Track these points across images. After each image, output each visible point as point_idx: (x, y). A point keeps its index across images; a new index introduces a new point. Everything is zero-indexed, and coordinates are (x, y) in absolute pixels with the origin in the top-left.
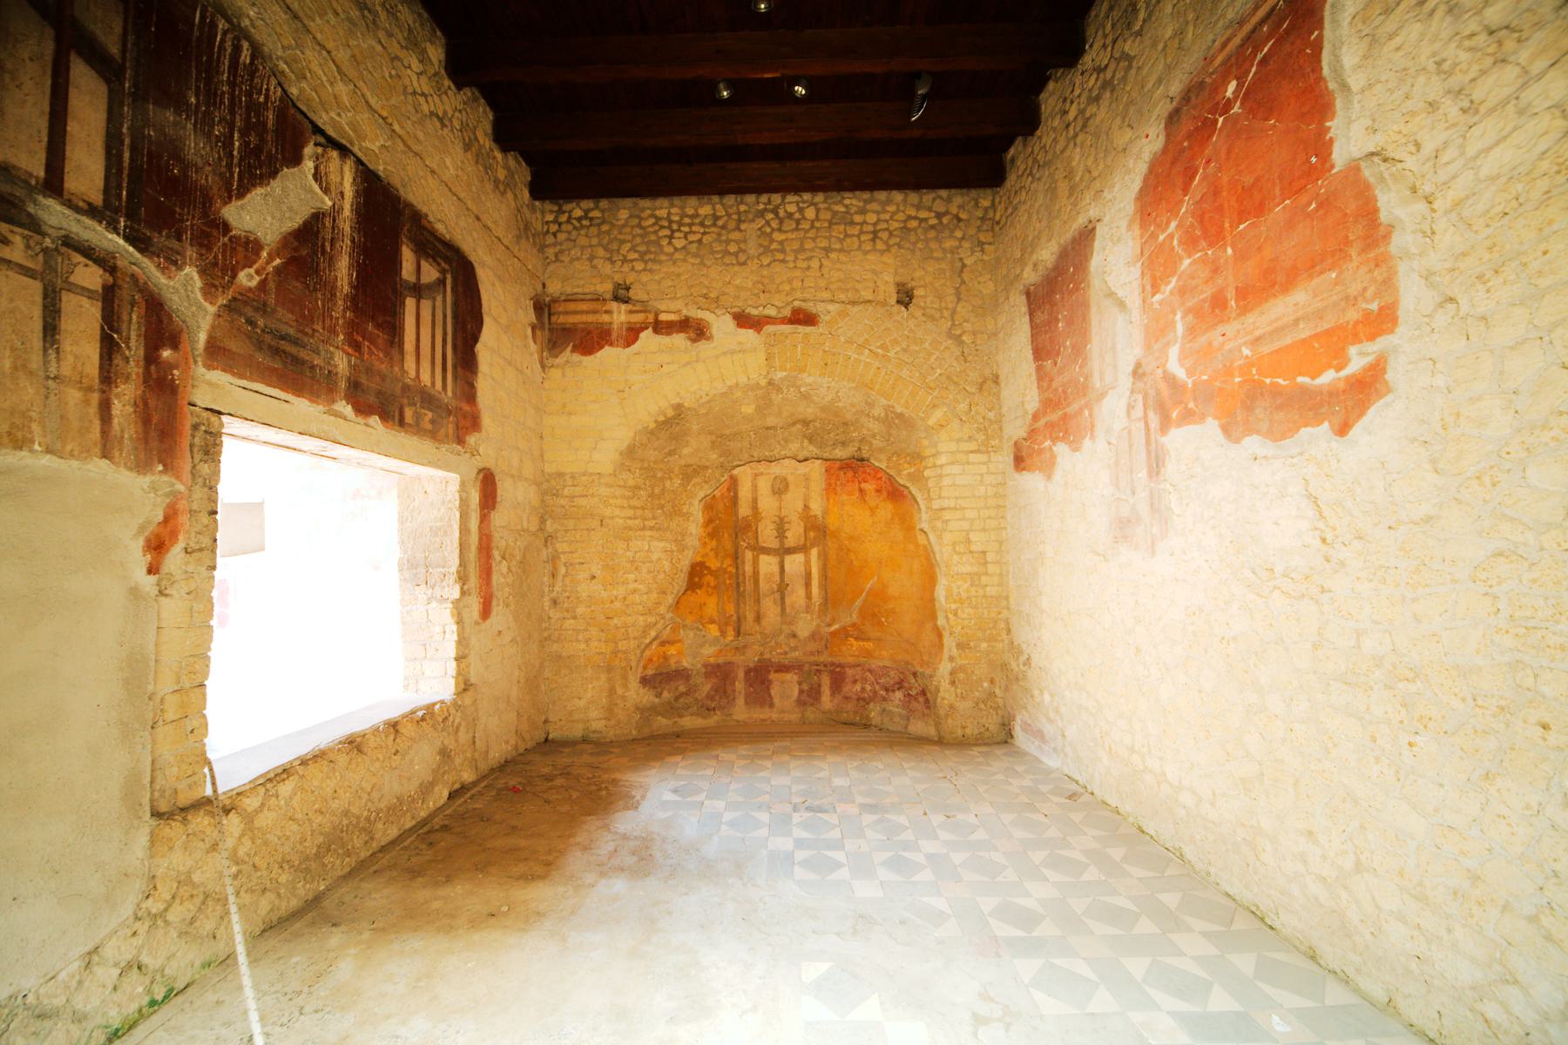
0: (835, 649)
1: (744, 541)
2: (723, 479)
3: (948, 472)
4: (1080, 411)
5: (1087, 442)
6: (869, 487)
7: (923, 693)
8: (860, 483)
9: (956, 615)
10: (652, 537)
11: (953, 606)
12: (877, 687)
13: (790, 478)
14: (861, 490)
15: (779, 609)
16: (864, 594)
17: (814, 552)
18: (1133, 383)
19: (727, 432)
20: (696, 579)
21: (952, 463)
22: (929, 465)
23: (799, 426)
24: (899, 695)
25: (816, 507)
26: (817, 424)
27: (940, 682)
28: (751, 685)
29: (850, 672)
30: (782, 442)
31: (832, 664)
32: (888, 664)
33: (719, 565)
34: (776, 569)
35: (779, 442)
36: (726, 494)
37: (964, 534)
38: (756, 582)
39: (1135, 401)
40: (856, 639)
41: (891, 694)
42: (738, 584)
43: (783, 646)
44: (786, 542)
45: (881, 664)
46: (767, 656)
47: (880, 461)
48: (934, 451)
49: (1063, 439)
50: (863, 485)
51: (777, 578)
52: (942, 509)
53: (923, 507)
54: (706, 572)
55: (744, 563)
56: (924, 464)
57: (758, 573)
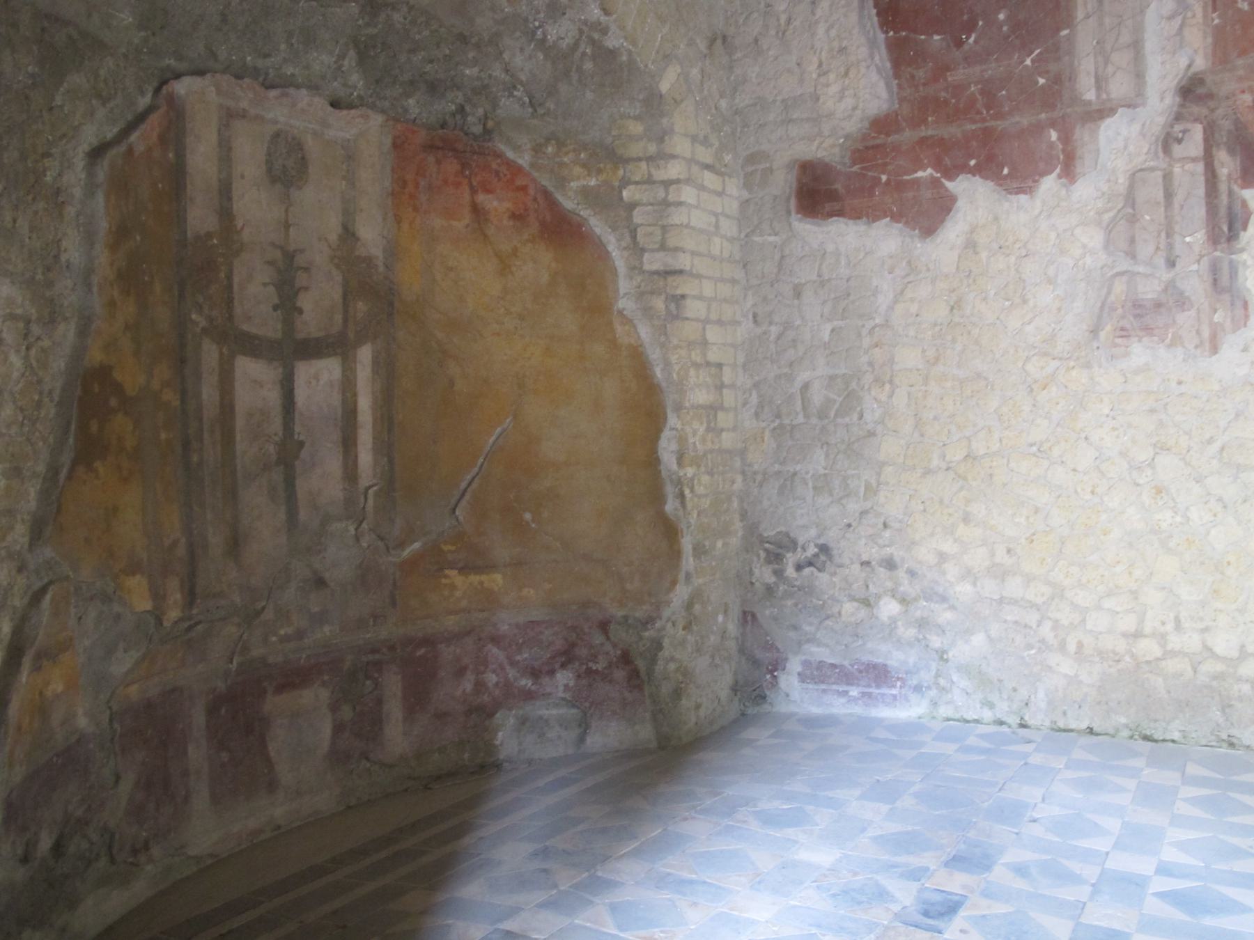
4: (1038, 129)
5: (1049, 184)
6: (496, 204)
7: (626, 658)
9: (692, 490)
12: (512, 673)
13: (311, 146)
14: (476, 209)
15: (282, 515)
17: (365, 354)
18: (1182, 106)
20: (94, 427)
24: (564, 678)
25: (371, 234)
27: (663, 628)
29: (447, 653)
34: (273, 396)
38: (228, 439)
39: (1184, 132)
41: (545, 680)
42: (186, 445)
45: (521, 619)
46: (256, 652)
47: (517, 148)
48: (652, 148)
49: (977, 171)
50: (481, 198)
51: (276, 426)
52: (668, 273)
56: (621, 172)
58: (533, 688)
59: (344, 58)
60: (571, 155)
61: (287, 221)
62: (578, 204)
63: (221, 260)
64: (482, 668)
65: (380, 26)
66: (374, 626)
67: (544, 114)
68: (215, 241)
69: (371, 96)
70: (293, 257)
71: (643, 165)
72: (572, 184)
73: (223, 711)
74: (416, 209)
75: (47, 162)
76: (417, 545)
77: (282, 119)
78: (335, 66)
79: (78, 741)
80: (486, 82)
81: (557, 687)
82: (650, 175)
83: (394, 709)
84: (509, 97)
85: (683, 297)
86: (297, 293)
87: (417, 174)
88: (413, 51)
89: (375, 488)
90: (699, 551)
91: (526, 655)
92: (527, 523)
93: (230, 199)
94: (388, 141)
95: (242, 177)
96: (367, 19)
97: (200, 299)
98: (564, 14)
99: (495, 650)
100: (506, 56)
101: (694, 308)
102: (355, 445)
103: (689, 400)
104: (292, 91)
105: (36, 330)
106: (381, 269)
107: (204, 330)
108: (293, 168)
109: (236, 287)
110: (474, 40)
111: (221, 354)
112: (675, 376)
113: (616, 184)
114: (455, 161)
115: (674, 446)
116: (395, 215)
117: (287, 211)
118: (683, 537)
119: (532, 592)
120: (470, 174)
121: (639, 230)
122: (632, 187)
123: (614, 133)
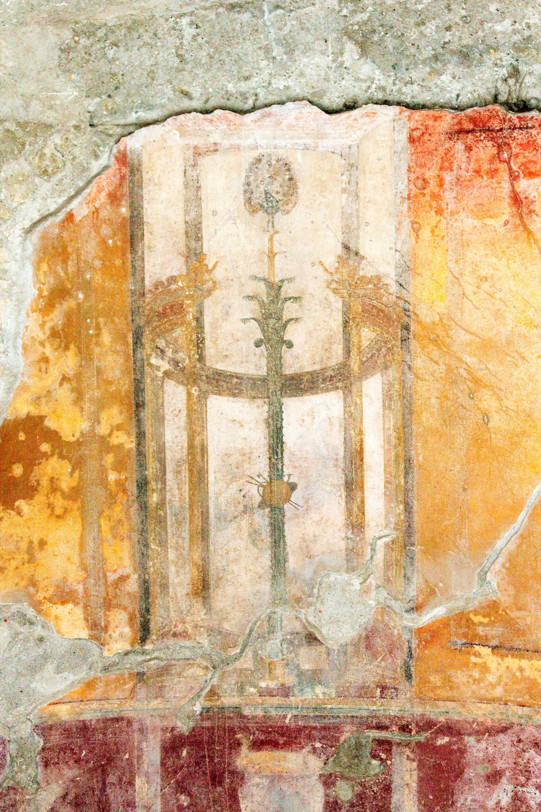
0: (435, 679)
2: (95, 166)
8: (514, 177)
15: (266, 559)
16: (523, 516)
28: (181, 788)
30: (277, 51)
33: (85, 426)
35: (267, 50)
36: (104, 214)
40: (494, 648)
43: (279, 671)
44: (288, 355)
54: (45, 447)
55: (160, 419)
57: (204, 450)
59: (342, 54)
61: (271, 251)
64: (522, 779)
65: (370, 9)
66: (382, 697)
68: (180, 284)
69: (394, 84)
73: (184, 753)
74: (439, 212)
77: (262, 142)
78: (334, 65)
80: (527, 33)
86: (285, 326)
87: (441, 169)
93: (199, 239)
94: (404, 137)
95: (214, 213)
96: (351, 6)
97: (162, 343)
102: (362, 488)
104: (275, 108)
106: (394, 288)
107: (167, 374)
108: (277, 193)
109: (207, 328)
111: (189, 394)
114: (490, 144)
116: (413, 223)
117: (271, 240)
120: (510, 158)
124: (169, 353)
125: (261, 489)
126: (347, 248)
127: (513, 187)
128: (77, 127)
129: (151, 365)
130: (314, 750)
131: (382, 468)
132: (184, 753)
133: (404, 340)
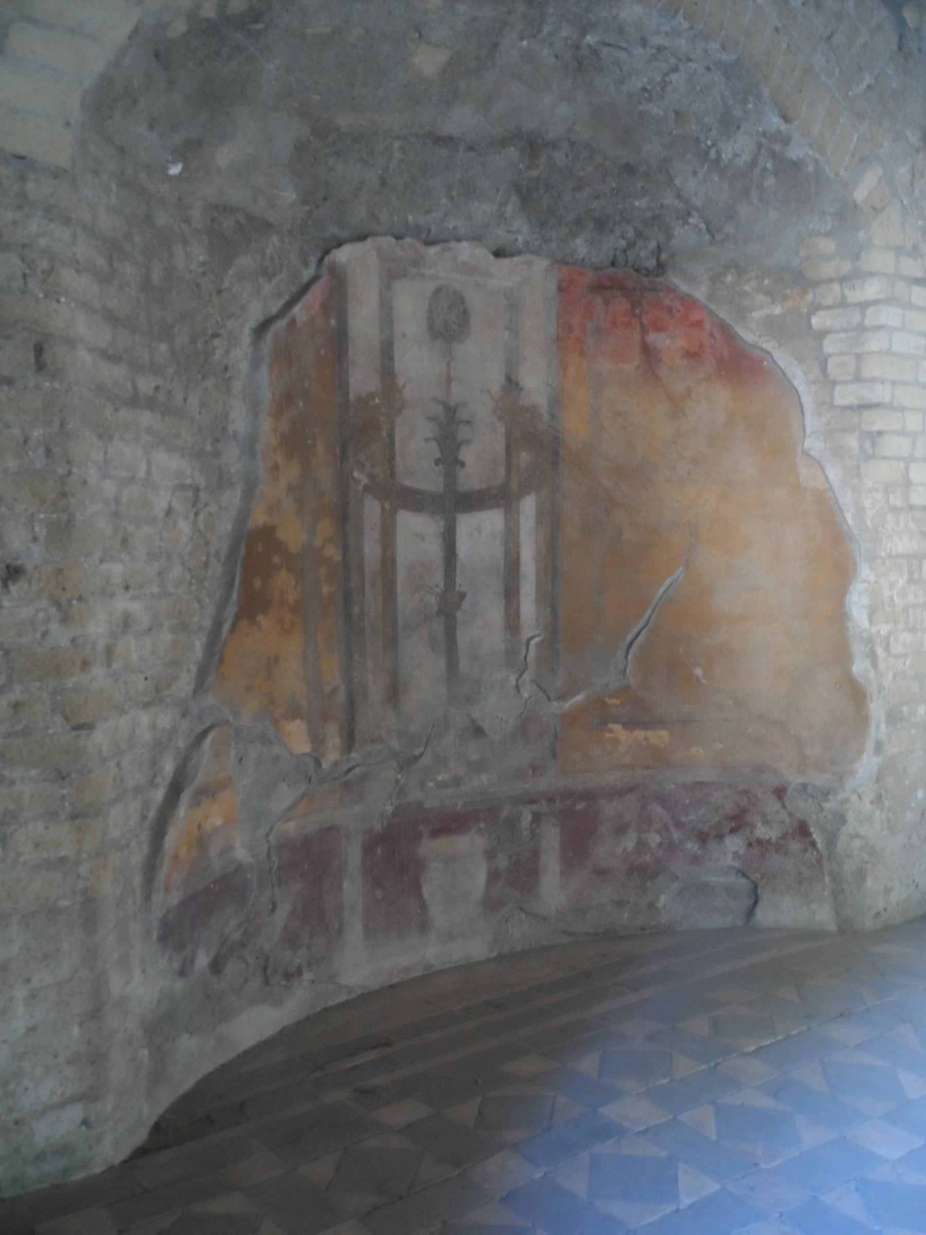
1: (362, 467)
3: (882, 321)
7: (803, 830)
8: (644, 330)
9: (887, 648)
10: (150, 431)
11: (884, 629)
12: (676, 834)
15: (442, 665)
17: (528, 505)
19: (345, 121)
20: (257, 583)
21: (887, 301)
22: (828, 302)
23: (513, 152)
24: (734, 844)
26: (559, 157)
27: (847, 801)
29: (609, 808)
31: (568, 795)
32: (706, 775)
34: (434, 549)
37: (902, 464)
41: (712, 845)
42: (347, 597)
46: (414, 796)
48: (847, 267)
50: (653, 338)
51: (438, 577)
52: (865, 407)
53: (808, 401)
56: (810, 297)
57: (393, 562)
58: (700, 852)
59: (506, 204)
60: (753, 283)
62: (760, 336)
63: (383, 419)
67: (723, 241)
70: (455, 411)
71: (836, 287)
72: (754, 314)
73: (379, 851)
74: (582, 353)
75: (216, 342)
76: (580, 698)
79: (236, 870)
81: (725, 854)
82: (843, 296)
83: (551, 863)
84: (683, 225)
85: (880, 433)
86: (458, 447)
88: (577, 188)
89: (537, 639)
90: (893, 717)
91: (692, 817)
92: (698, 678)
93: (391, 358)
94: (553, 286)
95: (404, 335)
97: (362, 458)
98: (738, 128)
99: (659, 809)
100: (678, 182)
101: (894, 445)
103: (885, 550)
104: (453, 244)
105: (203, 496)
106: (546, 418)
107: (366, 488)
110: (642, 170)
111: (383, 508)
112: (869, 522)
113: (805, 310)
114: (624, 300)
115: (865, 601)
117: (448, 366)
118: (872, 701)
119: (701, 750)
121: (830, 360)
122: (822, 313)
123: (802, 253)
124: (368, 466)
125: (438, 598)
126: (509, 379)
127: (643, 338)
128: (290, 232)
129: (354, 479)
130: (480, 830)
131: (534, 577)
132: (379, 851)
133: (555, 464)
